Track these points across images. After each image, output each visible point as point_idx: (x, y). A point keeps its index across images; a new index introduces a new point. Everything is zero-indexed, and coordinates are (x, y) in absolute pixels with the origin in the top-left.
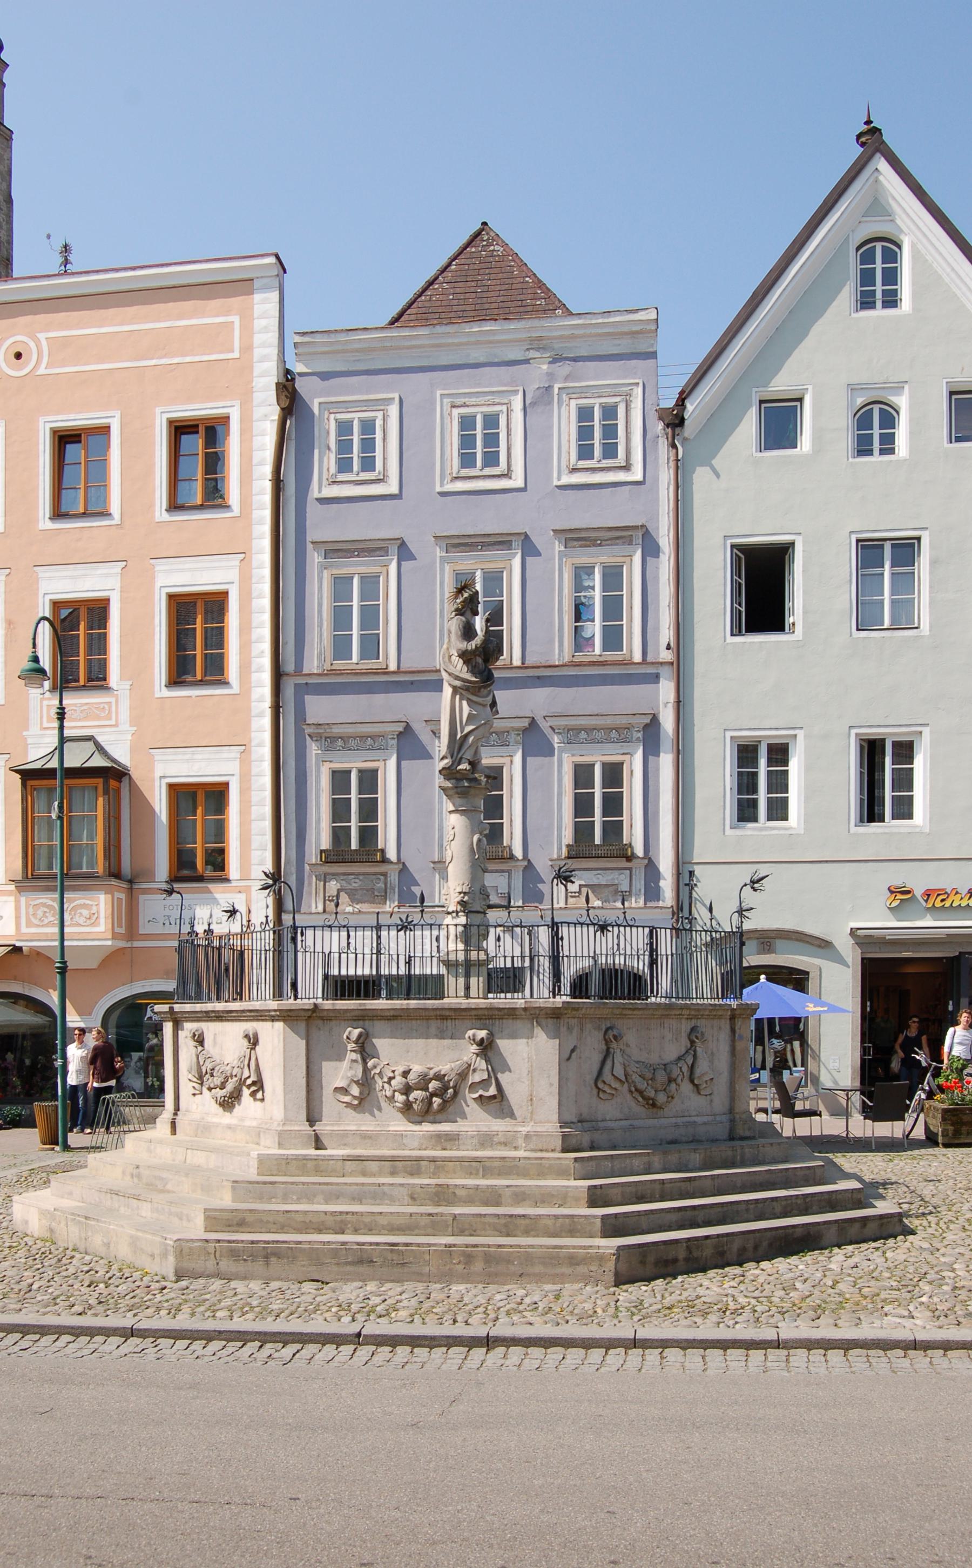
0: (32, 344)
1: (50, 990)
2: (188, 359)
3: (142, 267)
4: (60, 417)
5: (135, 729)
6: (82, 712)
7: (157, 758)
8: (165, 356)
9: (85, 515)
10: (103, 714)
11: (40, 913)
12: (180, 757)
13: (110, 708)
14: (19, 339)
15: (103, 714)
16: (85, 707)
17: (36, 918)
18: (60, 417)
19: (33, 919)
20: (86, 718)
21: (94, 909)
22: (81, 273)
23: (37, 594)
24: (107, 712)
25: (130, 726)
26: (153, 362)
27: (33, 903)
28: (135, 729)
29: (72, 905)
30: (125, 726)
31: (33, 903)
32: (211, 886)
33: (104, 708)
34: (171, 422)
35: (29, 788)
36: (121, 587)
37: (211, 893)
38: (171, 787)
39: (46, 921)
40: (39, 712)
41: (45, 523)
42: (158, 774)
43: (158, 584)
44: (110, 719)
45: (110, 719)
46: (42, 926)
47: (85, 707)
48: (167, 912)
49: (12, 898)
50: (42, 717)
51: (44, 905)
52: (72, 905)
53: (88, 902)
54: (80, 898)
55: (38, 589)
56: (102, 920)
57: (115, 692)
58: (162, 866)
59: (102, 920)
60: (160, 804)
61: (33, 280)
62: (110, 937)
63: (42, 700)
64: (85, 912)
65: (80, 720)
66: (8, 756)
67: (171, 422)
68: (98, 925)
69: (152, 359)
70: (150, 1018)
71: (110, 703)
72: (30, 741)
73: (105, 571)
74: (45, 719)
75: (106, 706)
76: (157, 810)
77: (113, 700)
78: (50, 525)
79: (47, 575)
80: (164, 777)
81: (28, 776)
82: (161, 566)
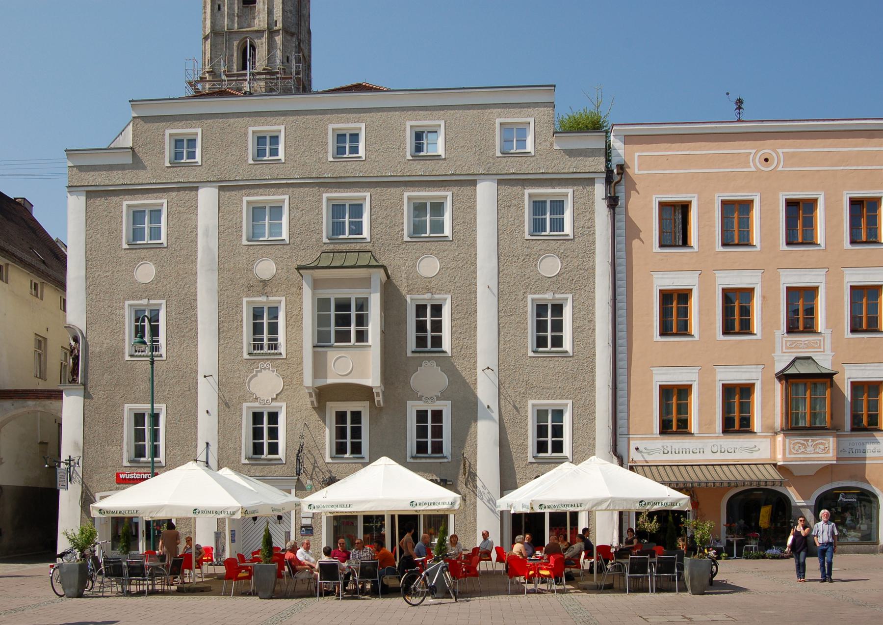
0: (774, 155)
1: (787, 487)
2: (860, 168)
3: (838, 120)
4: (791, 193)
5: (834, 353)
6: (805, 344)
7: (846, 368)
8: (847, 166)
9: (802, 244)
10: (816, 346)
11: (797, 447)
12: (859, 368)
13: (820, 342)
14: (766, 151)
15: (816, 346)
16: (807, 342)
17: (794, 450)
18: (791, 193)
19: (793, 450)
20: (806, 348)
21: (827, 445)
22: (800, 120)
23: (779, 284)
24: (818, 345)
25: (831, 352)
26: (841, 168)
27: (793, 442)
28: (834, 353)
29: (815, 443)
30: (828, 352)
31: (793, 442)
32: (874, 433)
33: (817, 342)
34: (850, 199)
35: (789, 383)
36: (826, 282)
37: (875, 436)
38: (852, 383)
39: (800, 451)
40: (781, 344)
41: (783, 246)
42: (846, 377)
43: (846, 281)
44: (821, 348)
45: (821, 348)
46: (798, 454)
47: (807, 342)
48: (851, 446)
49: (769, 440)
50: (782, 346)
51: (799, 443)
52: (815, 443)
53: (823, 441)
54: (819, 440)
55: (780, 281)
56: (831, 451)
57: (823, 335)
58: (848, 425)
59: (831, 451)
60: (847, 392)
61: (777, 122)
62: (835, 459)
63: (782, 338)
64: (822, 447)
65: (804, 348)
66: (764, 366)
67: (850, 199)
68: (829, 453)
69: (841, 166)
70: (841, 500)
71: (820, 340)
72: (776, 359)
73: (817, 273)
74: (784, 348)
75: (818, 342)
76: (846, 395)
77: (822, 339)
78: (786, 248)
79: (785, 273)
80: (850, 378)
81: (784, 377)
82: (847, 272)
